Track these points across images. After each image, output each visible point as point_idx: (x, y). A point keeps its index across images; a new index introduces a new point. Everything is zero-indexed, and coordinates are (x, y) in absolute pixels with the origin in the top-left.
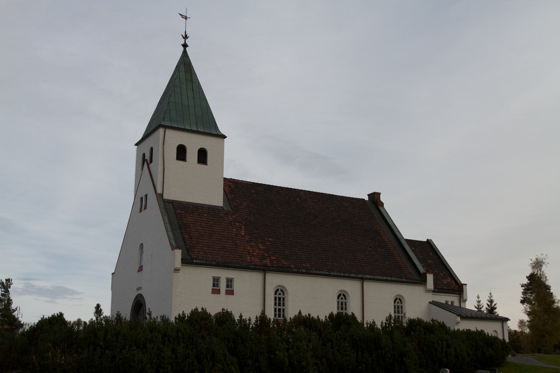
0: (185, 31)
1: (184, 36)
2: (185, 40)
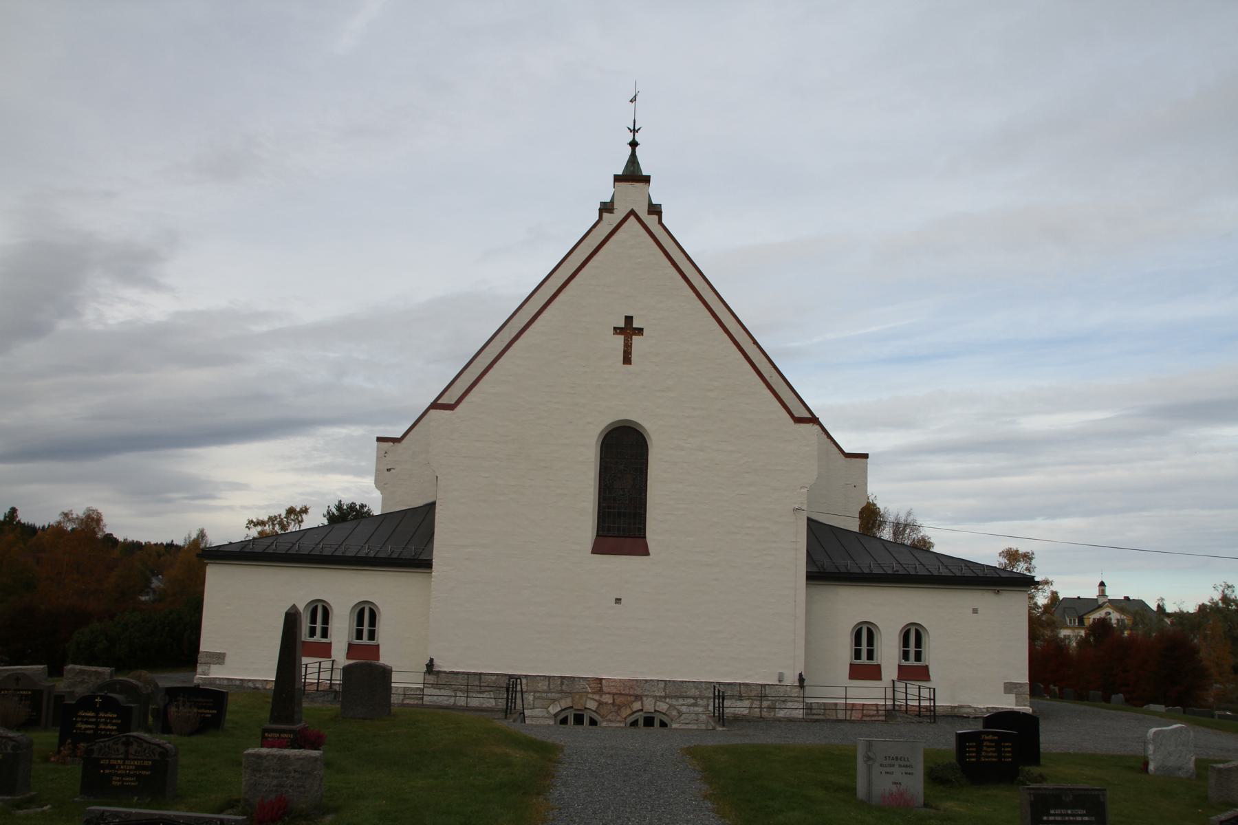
0: (635, 120)
1: (632, 128)
2: (634, 135)
